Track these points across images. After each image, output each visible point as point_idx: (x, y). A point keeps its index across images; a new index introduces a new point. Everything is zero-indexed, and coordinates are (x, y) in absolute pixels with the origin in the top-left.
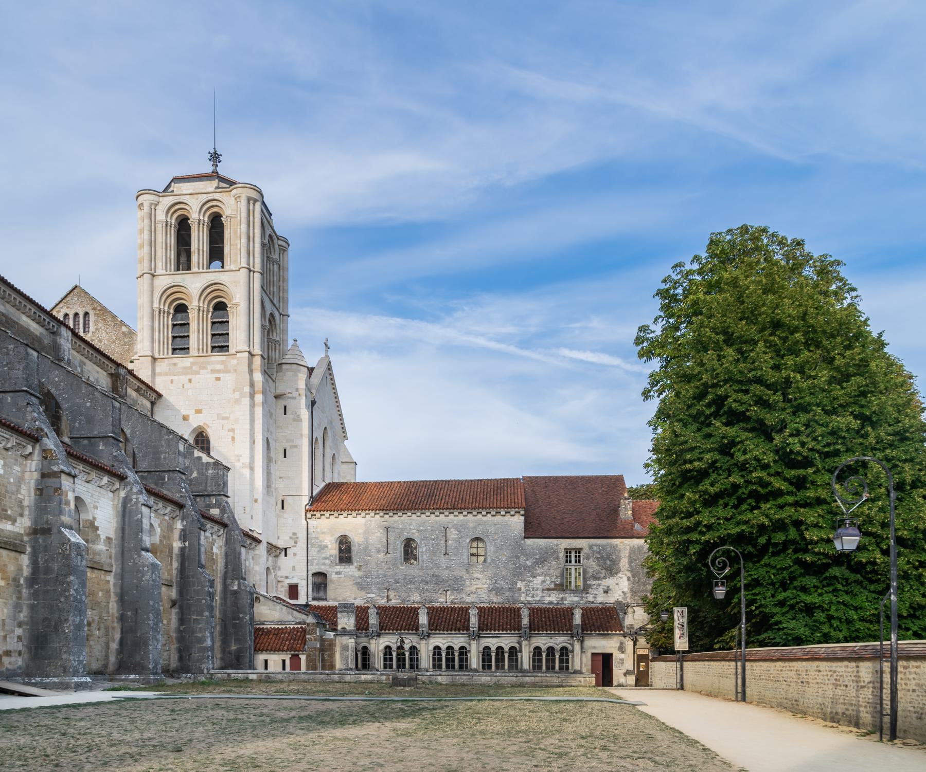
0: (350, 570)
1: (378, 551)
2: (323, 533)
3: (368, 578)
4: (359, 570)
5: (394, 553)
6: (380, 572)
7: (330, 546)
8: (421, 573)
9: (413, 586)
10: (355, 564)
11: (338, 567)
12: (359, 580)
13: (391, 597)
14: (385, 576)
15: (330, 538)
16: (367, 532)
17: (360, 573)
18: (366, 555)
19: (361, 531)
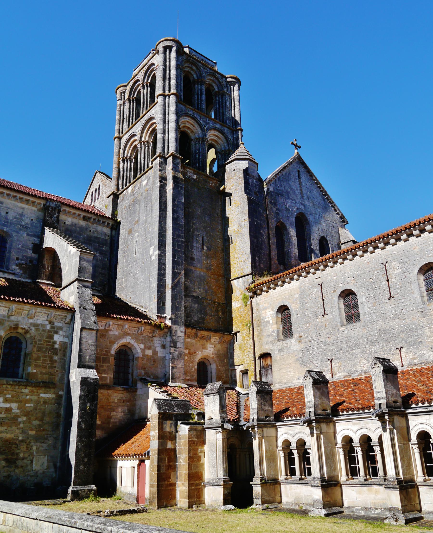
0: (292, 343)
1: (315, 315)
2: (265, 309)
3: (308, 350)
4: (300, 342)
5: (332, 312)
6: (321, 340)
7: (271, 322)
8: (366, 331)
9: (358, 351)
10: (296, 337)
11: (280, 343)
12: (300, 355)
13: (335, 369)
14: (326, 344)
15: (271, 312)
16: (303, 296)
17: (302, 346)
18: (304, 323)
19: (296, 296)
